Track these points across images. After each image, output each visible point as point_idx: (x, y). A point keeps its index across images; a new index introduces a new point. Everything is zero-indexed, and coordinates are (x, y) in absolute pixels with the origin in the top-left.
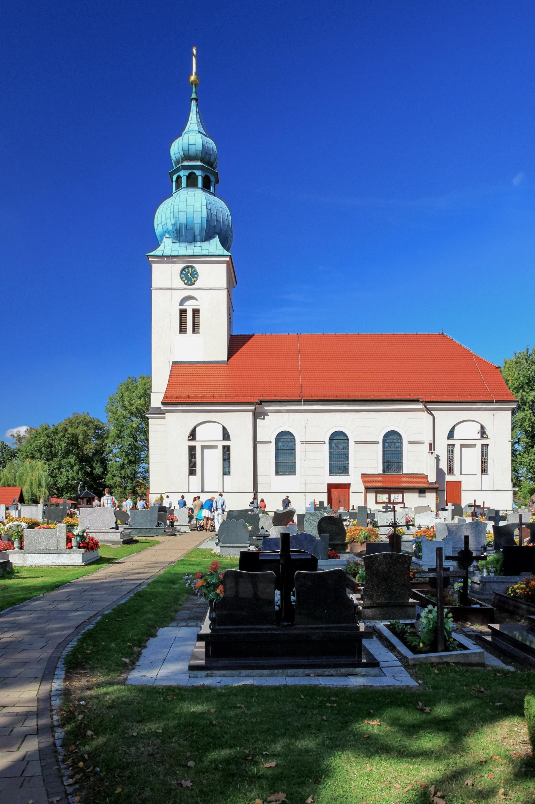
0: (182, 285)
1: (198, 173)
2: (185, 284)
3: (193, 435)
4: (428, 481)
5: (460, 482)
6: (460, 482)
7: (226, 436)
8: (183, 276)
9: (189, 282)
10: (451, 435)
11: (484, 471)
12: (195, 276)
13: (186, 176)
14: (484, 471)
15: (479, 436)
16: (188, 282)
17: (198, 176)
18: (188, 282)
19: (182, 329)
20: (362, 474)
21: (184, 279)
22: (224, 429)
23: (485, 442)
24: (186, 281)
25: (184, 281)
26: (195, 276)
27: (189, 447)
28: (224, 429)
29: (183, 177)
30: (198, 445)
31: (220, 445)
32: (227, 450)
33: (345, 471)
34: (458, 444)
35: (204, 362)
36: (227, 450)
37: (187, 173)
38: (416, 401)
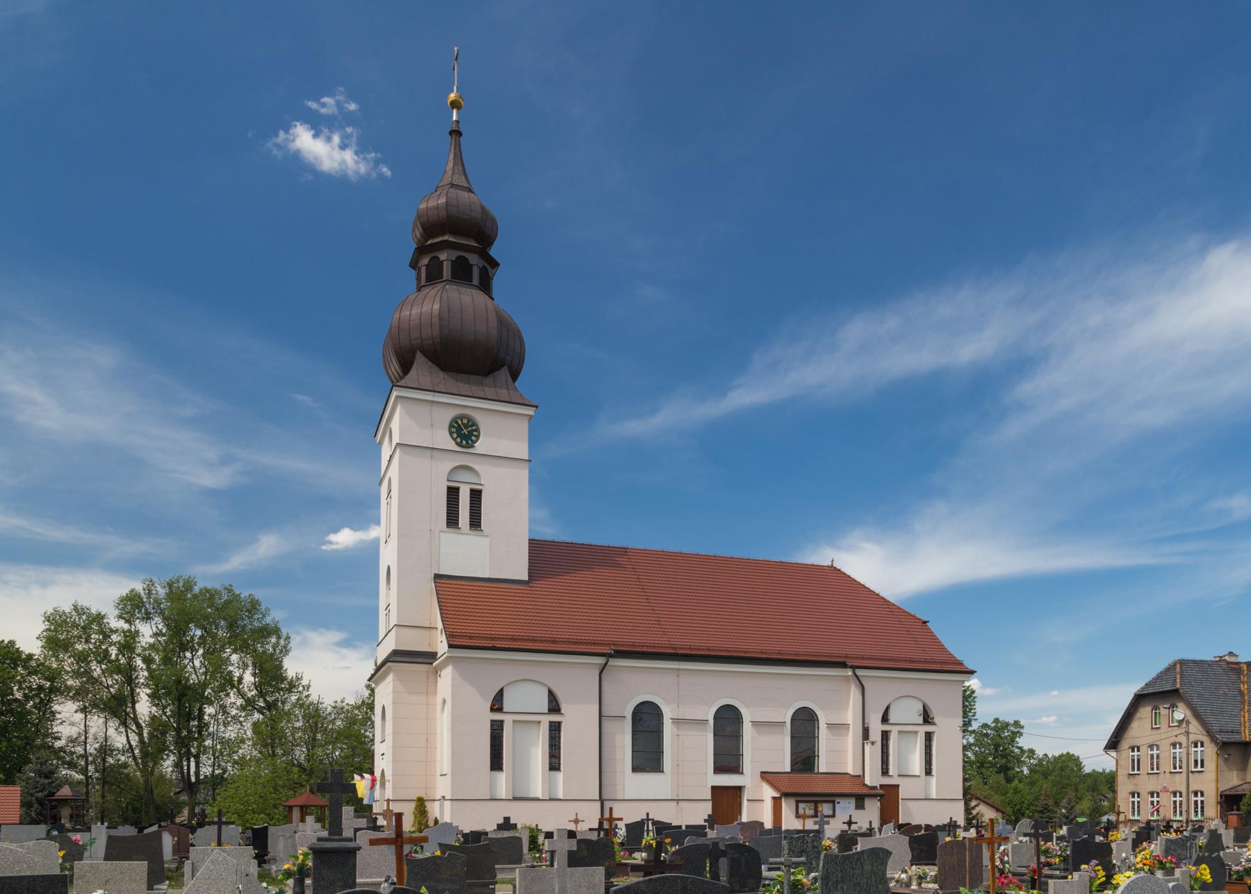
0: (452, 445)
1: (474, 259)
2: (457, 444)
3: (497, 704)
4: (865, 785)
5: (897, 786)
6: (897, 786)
7: (554, 707)
8: (454, 430)
9: (464, 442)
10: (885, 719)
11: (928, 772)
12: (475, 433)
13: (452, 261)
14: (928, 772)
15: (921, 720)
16: (461, 442)
17: (472, 265)
18: (461, 442)
19: (452, 521)
20: (761, 772)
21: (455, 435)
22: (551, 694)
23: (929, 728)
24: (459, 440)
25: (455, 440)
26: (475, 433)
27: (882, 732)
28: (551, 694)
29: (445, 263)
30: (508, 720)
31: (546, 720)
32: (555, 729)
33: (736, 769)
34: (894, 730)
35: (489, 578)
36: (555, 729)
37: (455, 254)
38: (843, 665)
